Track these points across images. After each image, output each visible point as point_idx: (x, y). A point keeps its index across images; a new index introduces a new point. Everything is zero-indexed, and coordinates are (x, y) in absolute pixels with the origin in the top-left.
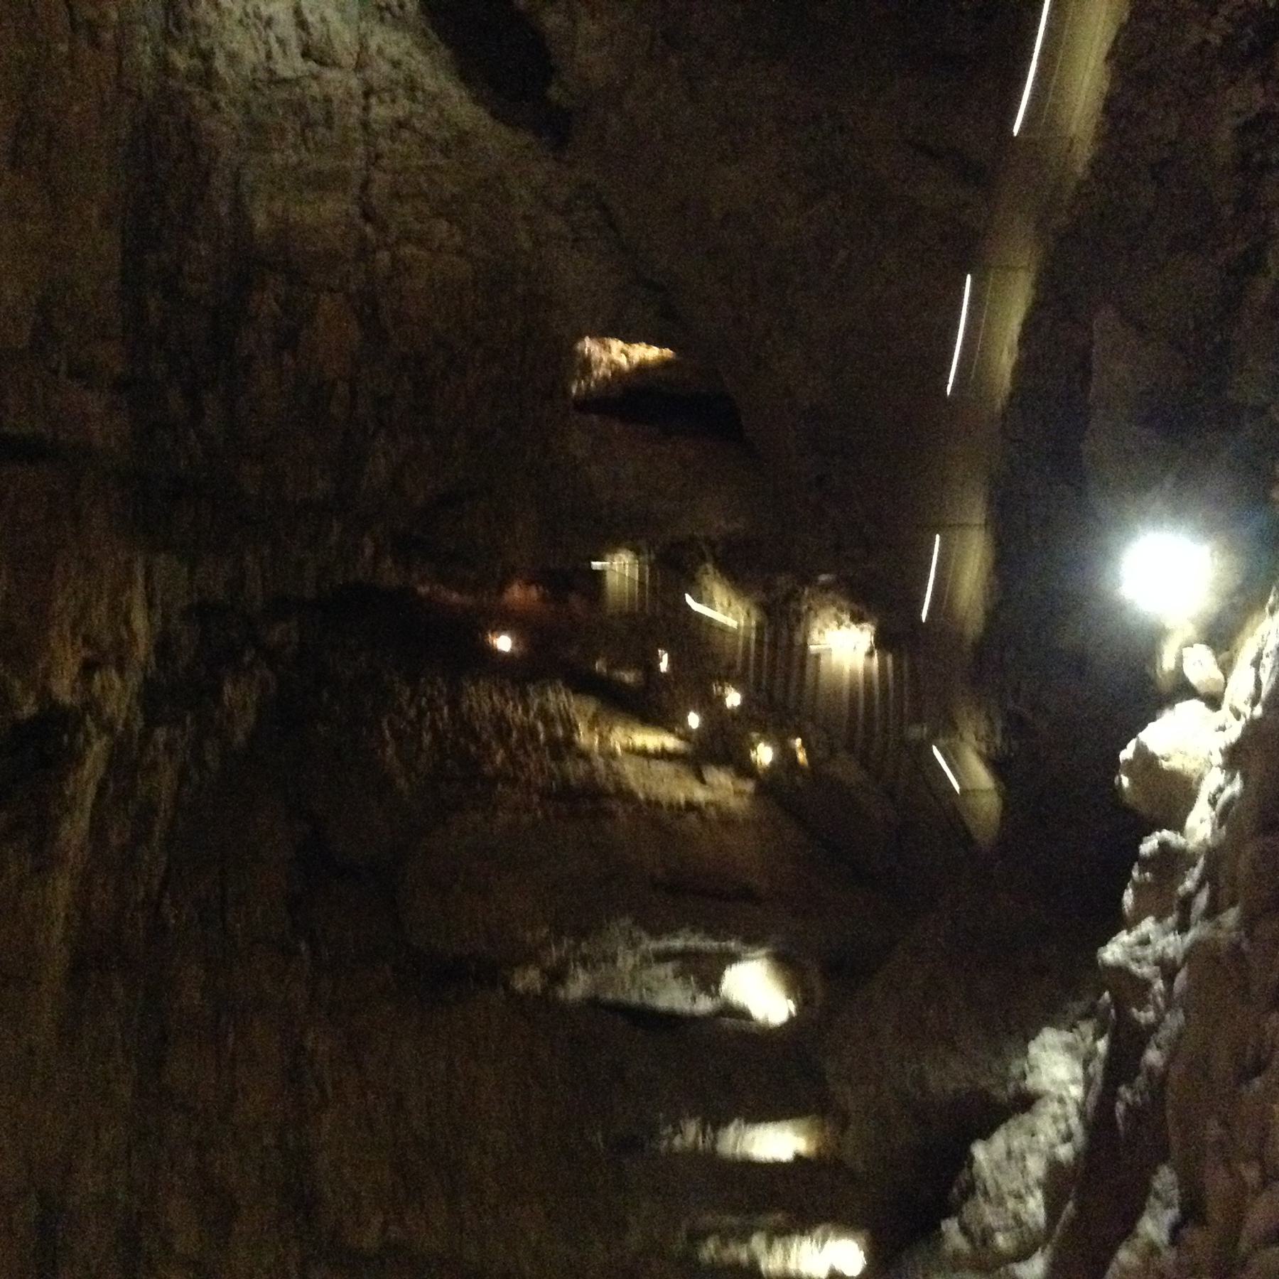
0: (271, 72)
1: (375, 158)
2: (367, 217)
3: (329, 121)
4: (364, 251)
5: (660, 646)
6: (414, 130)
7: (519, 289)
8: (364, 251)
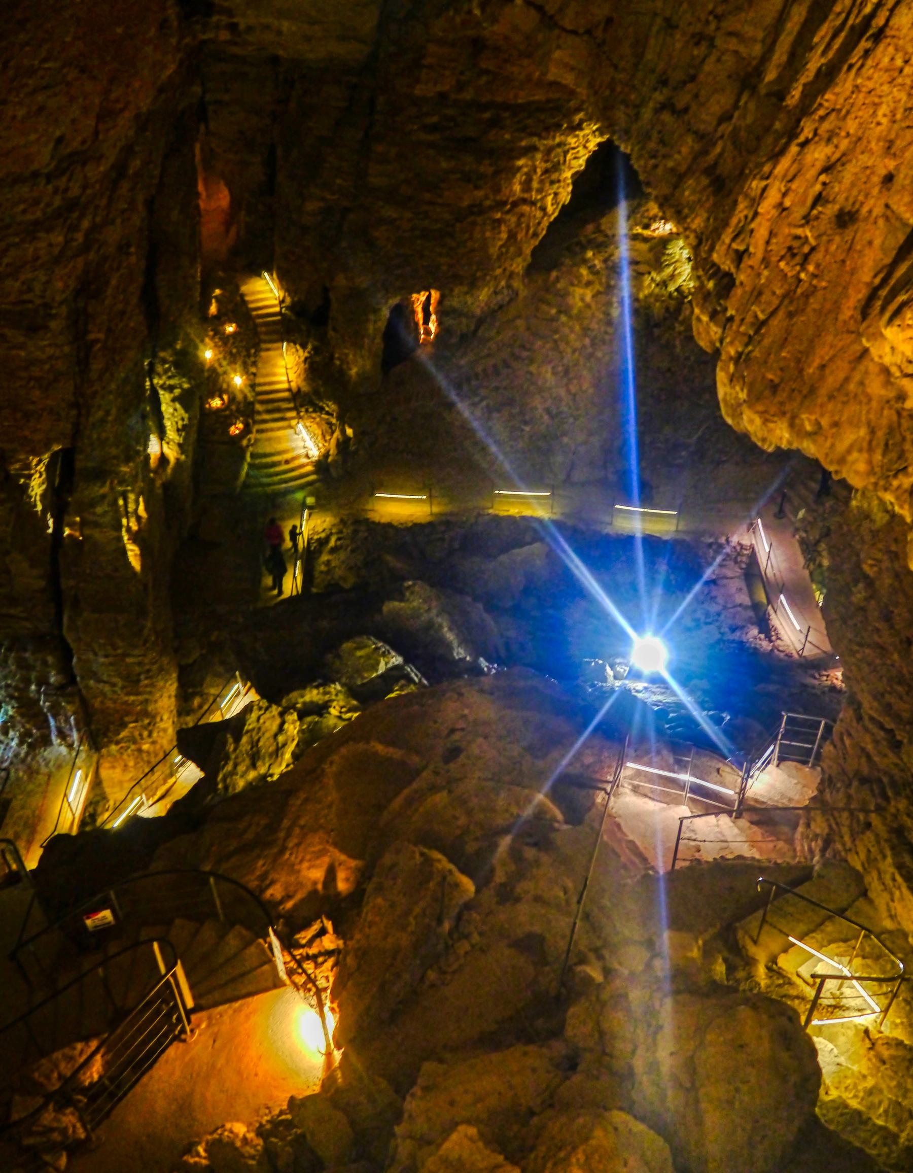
0: (568, 151)
1: (533, 203)
2: (515, 204)
3: (552, 183)
5: (238, 326)
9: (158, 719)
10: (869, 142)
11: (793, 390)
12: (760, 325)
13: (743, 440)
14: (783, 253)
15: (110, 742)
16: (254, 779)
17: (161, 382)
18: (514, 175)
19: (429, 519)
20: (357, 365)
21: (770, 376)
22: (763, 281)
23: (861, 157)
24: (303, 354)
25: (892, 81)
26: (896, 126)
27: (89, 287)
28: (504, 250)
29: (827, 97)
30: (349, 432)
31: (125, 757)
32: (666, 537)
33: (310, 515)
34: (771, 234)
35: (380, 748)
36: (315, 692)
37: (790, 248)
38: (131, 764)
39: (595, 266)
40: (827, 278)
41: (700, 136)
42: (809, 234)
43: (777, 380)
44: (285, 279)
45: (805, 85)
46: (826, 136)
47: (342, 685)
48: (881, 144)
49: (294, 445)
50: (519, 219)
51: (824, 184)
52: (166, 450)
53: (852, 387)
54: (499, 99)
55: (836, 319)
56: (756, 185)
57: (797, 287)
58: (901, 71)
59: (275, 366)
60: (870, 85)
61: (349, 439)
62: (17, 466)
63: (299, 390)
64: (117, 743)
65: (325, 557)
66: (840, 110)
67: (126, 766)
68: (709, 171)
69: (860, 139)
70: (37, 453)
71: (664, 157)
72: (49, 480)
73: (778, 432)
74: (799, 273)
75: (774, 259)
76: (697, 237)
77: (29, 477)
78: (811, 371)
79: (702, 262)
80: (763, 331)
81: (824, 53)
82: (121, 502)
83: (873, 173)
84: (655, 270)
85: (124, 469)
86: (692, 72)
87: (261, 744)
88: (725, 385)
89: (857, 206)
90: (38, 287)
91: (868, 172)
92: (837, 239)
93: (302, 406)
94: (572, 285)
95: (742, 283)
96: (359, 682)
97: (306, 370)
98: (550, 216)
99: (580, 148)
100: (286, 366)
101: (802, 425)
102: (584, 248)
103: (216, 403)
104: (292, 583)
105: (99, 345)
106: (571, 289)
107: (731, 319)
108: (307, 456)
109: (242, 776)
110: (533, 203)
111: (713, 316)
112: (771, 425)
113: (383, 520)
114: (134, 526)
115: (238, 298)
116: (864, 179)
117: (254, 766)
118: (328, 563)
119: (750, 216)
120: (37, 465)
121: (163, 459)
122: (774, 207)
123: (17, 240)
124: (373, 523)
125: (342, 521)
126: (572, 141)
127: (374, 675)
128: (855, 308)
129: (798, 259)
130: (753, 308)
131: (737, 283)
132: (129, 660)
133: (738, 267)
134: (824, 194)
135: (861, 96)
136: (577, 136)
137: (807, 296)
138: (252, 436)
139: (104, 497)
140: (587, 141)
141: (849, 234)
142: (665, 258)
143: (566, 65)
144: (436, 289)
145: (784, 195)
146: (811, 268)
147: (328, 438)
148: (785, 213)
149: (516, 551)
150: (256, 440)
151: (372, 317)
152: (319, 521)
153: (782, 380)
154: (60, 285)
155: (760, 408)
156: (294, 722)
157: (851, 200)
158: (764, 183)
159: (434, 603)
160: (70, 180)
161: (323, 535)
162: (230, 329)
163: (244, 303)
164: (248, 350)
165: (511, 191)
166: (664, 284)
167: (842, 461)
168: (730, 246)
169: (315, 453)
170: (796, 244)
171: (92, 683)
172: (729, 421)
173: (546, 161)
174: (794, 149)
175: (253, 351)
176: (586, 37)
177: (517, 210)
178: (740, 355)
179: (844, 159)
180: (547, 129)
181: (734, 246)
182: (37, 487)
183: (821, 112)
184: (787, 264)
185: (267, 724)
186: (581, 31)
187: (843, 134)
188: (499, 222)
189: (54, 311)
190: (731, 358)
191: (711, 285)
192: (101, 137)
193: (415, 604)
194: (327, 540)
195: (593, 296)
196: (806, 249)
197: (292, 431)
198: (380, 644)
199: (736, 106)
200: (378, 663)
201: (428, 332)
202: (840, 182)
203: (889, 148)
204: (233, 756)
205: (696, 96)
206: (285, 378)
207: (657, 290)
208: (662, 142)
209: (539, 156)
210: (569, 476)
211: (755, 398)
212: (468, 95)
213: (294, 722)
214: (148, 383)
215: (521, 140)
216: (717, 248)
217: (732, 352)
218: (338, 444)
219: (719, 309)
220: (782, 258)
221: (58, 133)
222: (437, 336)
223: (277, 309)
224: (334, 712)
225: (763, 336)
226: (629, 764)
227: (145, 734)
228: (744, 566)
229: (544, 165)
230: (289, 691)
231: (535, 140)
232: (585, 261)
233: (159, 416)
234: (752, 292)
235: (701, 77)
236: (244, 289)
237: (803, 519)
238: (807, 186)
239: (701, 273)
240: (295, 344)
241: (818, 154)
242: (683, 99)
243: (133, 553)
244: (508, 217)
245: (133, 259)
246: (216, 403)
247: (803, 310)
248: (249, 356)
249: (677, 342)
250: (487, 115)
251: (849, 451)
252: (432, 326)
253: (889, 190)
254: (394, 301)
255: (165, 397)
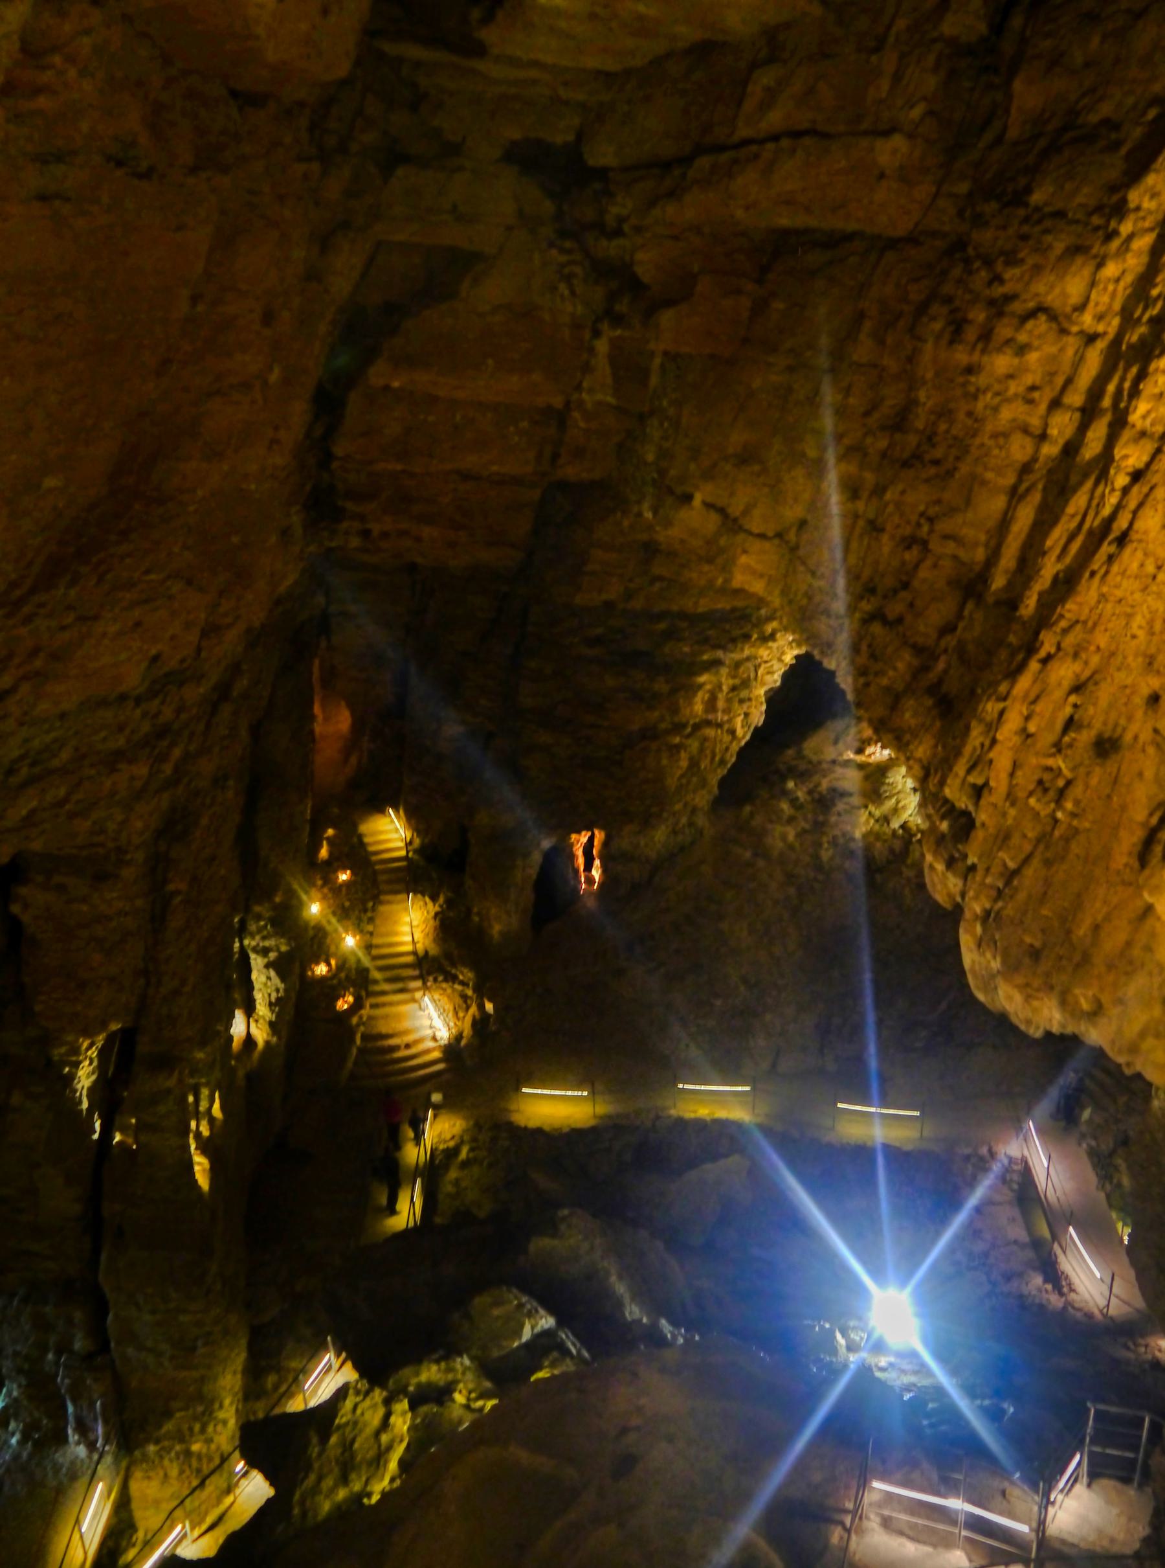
0: (760, 665)
1: (719, 725)
2: (697, 727)
3: (741, 701)
4: (678, 728)
5: (353, 873)
6: (731, 742)
7: (654, 810)
8: (678, 728)
9: (216, 1406)
10: (1125, 658)
11: (1061, 958)
12: (1011, 876)
13: (1002, 1021)
14: (1031, 787)
15: (147, 1441)
16: (345, 1500)
17: (253, 943)
18: (695, 694)
19: (592, 1123)
20: (501, 921)
21: (1028, 940)
22: (1010, 822)
23: (1116, 674)
24: (433, 908)
25: (1145, 589)
26: (1155, 639)
27: (174, 827)
28: (684, 781)
29: (1069, 606)
30: (489, 1007)
31: (166, 1462)
32: (908, 1147)
33: (435, 1116)
34: (1015, 765)
35: (523, 1456)
36: (434, 1368)
37: (1040, 782)
38: (174, 1472)
39: (797, 799)
40: (1091, 818)
41: (918, 650)
42: (1063, 766)
43: (1037, 944)
44: (414, 817)
45: (1041, 594)
46: (1071, 651)
47: (472, 1359)
48: (1140, 660)
49: (417, 1023)
50: (702, 744)
51: (1075, 706)
52: (254, 1030)
53: (1136, 952)
54: (675, 608)
55: (1107, 868)
56: (991, 708)
57: (1053, 829)
58: (1154, 577)
59: (396, 923)
60: (1119, 593)
61: (490, 1015)
62: (63, 1050)
63: (426, 952)
64: (157, 1442)
65: (453, 1174)
66: (1085, 622)
67: (166, 1476)
68: (933, 689)
69: (1113, 654)
70: (88, 1032)
71: (876, 674)
72: (102, 1069)
73: (1046, 1012)
74: (1054, 811)
75: (1021, 794)
76: (923, 767)
77: (77, 1065)
78: (1081, 932)
79: (931, 797)
80: (1015, 882)
81: (1060, 558)
82: (191, 1099)
83: (1133, 693)
84: (873, 802)
85: (200, 1055)
86: (904, 578)
87: (356, 1445)
88: (971, 951)
89: (1119, 730)
90: (111, 826)
91: (1128, 691)
92: (1098, 770)
93: (429, 974)
94: (771, 821)
95: (983, 825)
96: (495, 1353)
97: (435, 929)
98: (740, 740)
99: (774, 662)
100: (411, 924)
101: (1077, 1003)
102: (784, 778)
103: (321, 969)
104: (408, 1210)
105: (179, 899)
106: (770, 826)
107: (973, 868)
108: (434, 1039)
109: (327, 1496)
110: (719, 725)
111: (950, 863)
112: (1036, 1003)
113: (533, 1124)
114: (205, 1131)
115: (355, 840)
116: (1124, 700)
117: (344, 1480)
118: (457, 1182)
119: (987, 743)
120: (88, 1049)
121: (249, 1041)
122: (1016, 733)
123: (93, 772)
124: (519, 1128)
125: (478, 1126)
126: (763, 653)
127: (516, 1344)
128: (1130, 854)
129: (1052, 794)
130: (1001, 854)
131: (978, 824)
132: (184, 1318)
133: (977, 804)
134: (1076, 717)
135: (1109, 606)
136: (770, 648)
137: (1067, 840)
138: (365, 1012)
139: (169, 1091)
140: (783, 653)
141: (1111, 766)
142: (886, 787)
143: (754, 572)
144: (601, 828)
145: (1028, 718)
146: (1069, 805)
147: (461, 1014)
148: (1029, 741)
149: (708, 1166)
150: (370, 1018)
151: (519, 862)
152: (447, 1125)
153: (1044, 945)
154: (139, 824)
155: (1020, 980)
156: (404, 1413)
157: (1110, 726)
158: (1001, 705)
159: (598, 1241)
160: (163, 703)
161: (452, 1144)
162: (344, 877)
163: (362, 844)
164: (364, 902)
165: (692, 711)
166: (886, 819)
167: (1133, 1049)
168: (964, 781)
169: (444, 1035)
170: (1047, 777)
171: (130, 1351)
172: (981, 996)
173: (734, 677)
174: (1034, 665)
175: (370, 904)
176: (776, 541)
177: (699, 734)
178: (987, 913)
179: (1097, 677)
180: (734, 640)
181: (971, 779)
182: (85, 1077)
183: (1063, 624)
184: (1038, 800)
185: (367, 1416)
186: (770, 534)
187: (1092, 648)
188: (678, 747)
189: (129, 857)
190: (976, 917)
191: (944, 826)
192: (203, 654)
193: (572, 1241)
194: (456, 1151)
195: (798, 835)
196: (1061, 783)
197: (416, 1006)
198: (524, 1299)
199: (960, 616)
200: (522, 1326)
201: (590, 881)
202: (1095, 704)
203: (1150, 664)
204: (316, 1465)
205: (911, 605)
206: (409, 939)
207: (877, 827)
208: (873, 656)
209: (724, 671)
210: (774, 1066)
211: (1011, 968)
212: (638, 604)
213: (404, 1413)
214: (237, 945)
215: (703, 653)
216: (949, 781)
217: (978, 910)
218: (474, 1023)
219: (957, 855)
220: (1031, 794)
221: (153, 652)
222: (601, 885)
223: (403, 853)
224: (459, 1398)
225: (1016, 889)
226: (876, 1484)
227: (197, 1427)
228: (1015, 1187)
229: (731, 682)
230: (398, 1366)
231: (720, 654)
232: (785, 793)
233: (249, 986)
234: (996, 837)
235: (916, 583)
236: (364, 828)
237: (1090, 1121)
238: (1054, 710)
239: (931, 811)
240: (424, 896)
241: (1064, 672)
242: (895, 609)
243: (201, 1165)
244: (689, 741)
245: (230, 794)
246: (321, 969)
247: (1063, 858)
248: (365, 911)
249: (907, 891)
250: (662, 626)
251: (1143, 1035)
252: (596, 873)
253: (1156, 712)
254: (546, 844)
255: (257, 962)
